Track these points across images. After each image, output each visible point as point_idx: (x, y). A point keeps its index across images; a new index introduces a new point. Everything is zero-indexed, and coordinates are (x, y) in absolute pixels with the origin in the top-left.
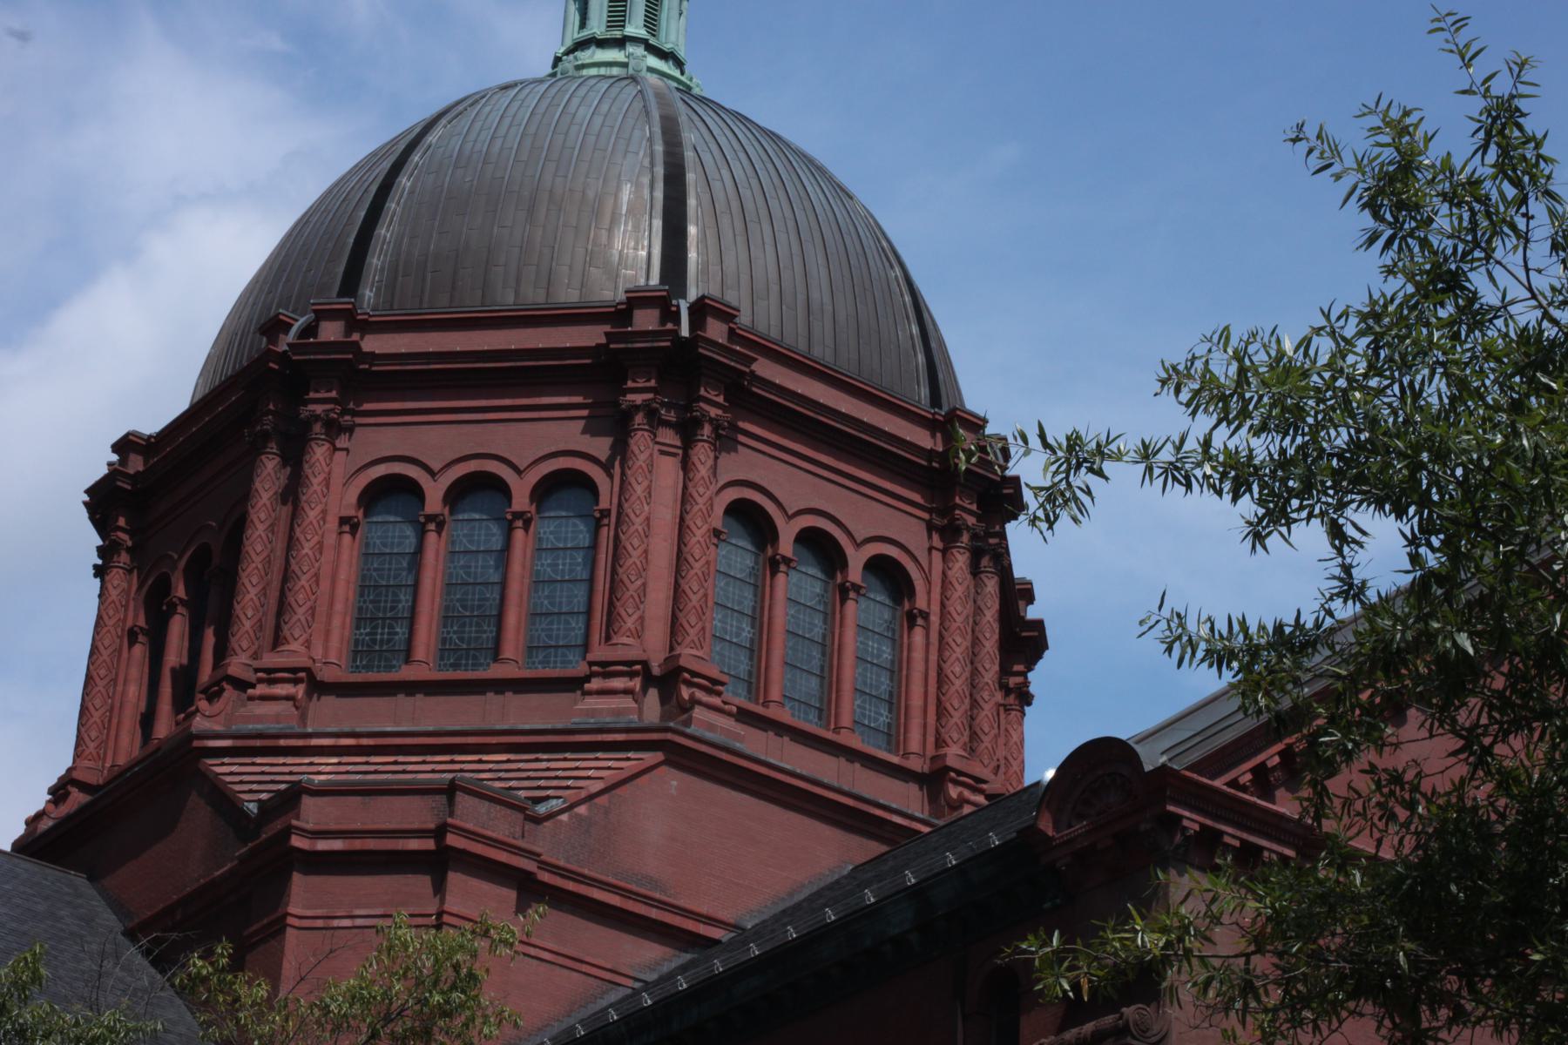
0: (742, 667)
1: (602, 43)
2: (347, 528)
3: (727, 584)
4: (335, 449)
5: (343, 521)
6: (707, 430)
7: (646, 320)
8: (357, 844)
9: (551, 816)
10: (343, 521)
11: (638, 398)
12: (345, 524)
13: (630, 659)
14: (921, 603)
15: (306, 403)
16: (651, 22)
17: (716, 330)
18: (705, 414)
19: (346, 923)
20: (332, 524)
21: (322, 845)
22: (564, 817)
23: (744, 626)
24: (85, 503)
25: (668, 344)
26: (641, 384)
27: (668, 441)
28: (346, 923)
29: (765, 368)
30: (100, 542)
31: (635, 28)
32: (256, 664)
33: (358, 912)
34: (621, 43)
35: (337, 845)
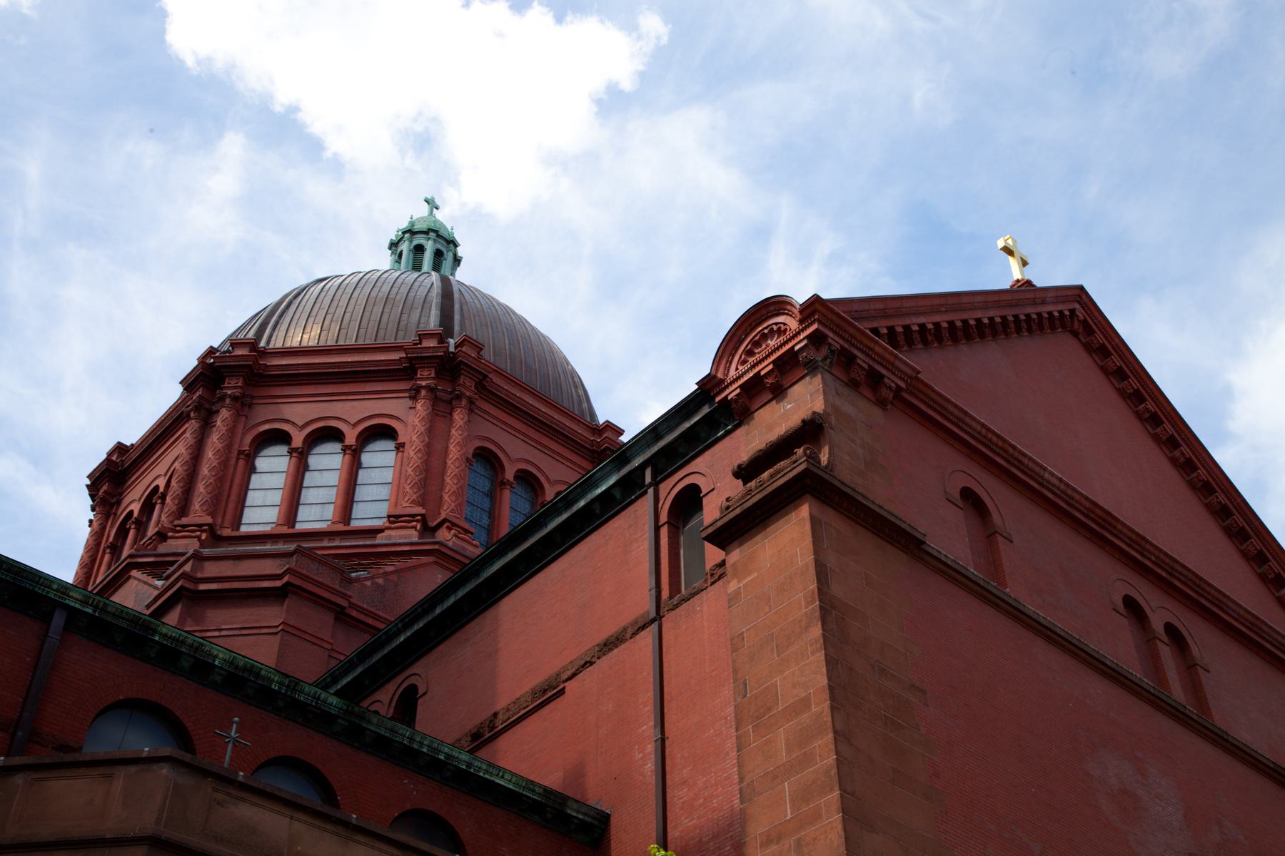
0: (482, 538)
2: (242, 456)
3: (475, 493)
4: (239, 415)
5: (240, 452)
6: (464, 402)
7: (432, 343)
8: (227, 586)
9: (358, 580)
10: (240, 452)
11: (424, 383)
12: (242, 454)
13: (414, 513)
15: (222, 389)
18: (463, 394)
19: (217, 634)
20: (235, 454)
21: (202, 587)
22: (368, 583)
23: (484, 517)
24: (87, 486)
25: (442, 354)
26: (426, 374)
27: (441, 409)
28: (217, 634)
30: (91, 503)
32: (176, 522)
33: (223, 627)
35: (214, 586)
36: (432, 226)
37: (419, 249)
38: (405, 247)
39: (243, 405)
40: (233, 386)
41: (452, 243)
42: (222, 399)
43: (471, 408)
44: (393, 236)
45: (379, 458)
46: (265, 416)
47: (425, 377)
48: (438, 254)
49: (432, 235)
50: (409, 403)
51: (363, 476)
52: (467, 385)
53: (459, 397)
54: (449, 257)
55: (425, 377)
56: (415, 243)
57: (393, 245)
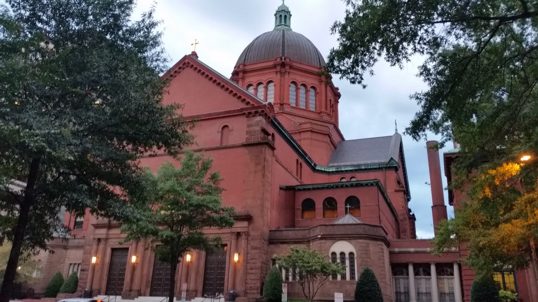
1: (279, 26)
6: (287, 73)
11: (278, 70)
14: (318, 91)
16: (285, 22)
17: (288, 60)
29: (294, 64)
31: (283, 23)
34: (281, 25)
36: (284, 9)
37: (281, 16)
38: (278, 16)
39: (243, 79)
40: (241, 75)
41: (289, 12)
42: (239, 78)
43: (289, 73)
44: (275, 13)
45: (271, 87)
46: (248, 81)
47: (278, 68)
48: (285, 17)
49: (283, 12)
50: (276, 75)
51: (268, 93)
52: (287, 68)
53: (286, 72)
54: (288, 16)
55: (278, 68)
56: (280, 14)
57: (275, 15)
